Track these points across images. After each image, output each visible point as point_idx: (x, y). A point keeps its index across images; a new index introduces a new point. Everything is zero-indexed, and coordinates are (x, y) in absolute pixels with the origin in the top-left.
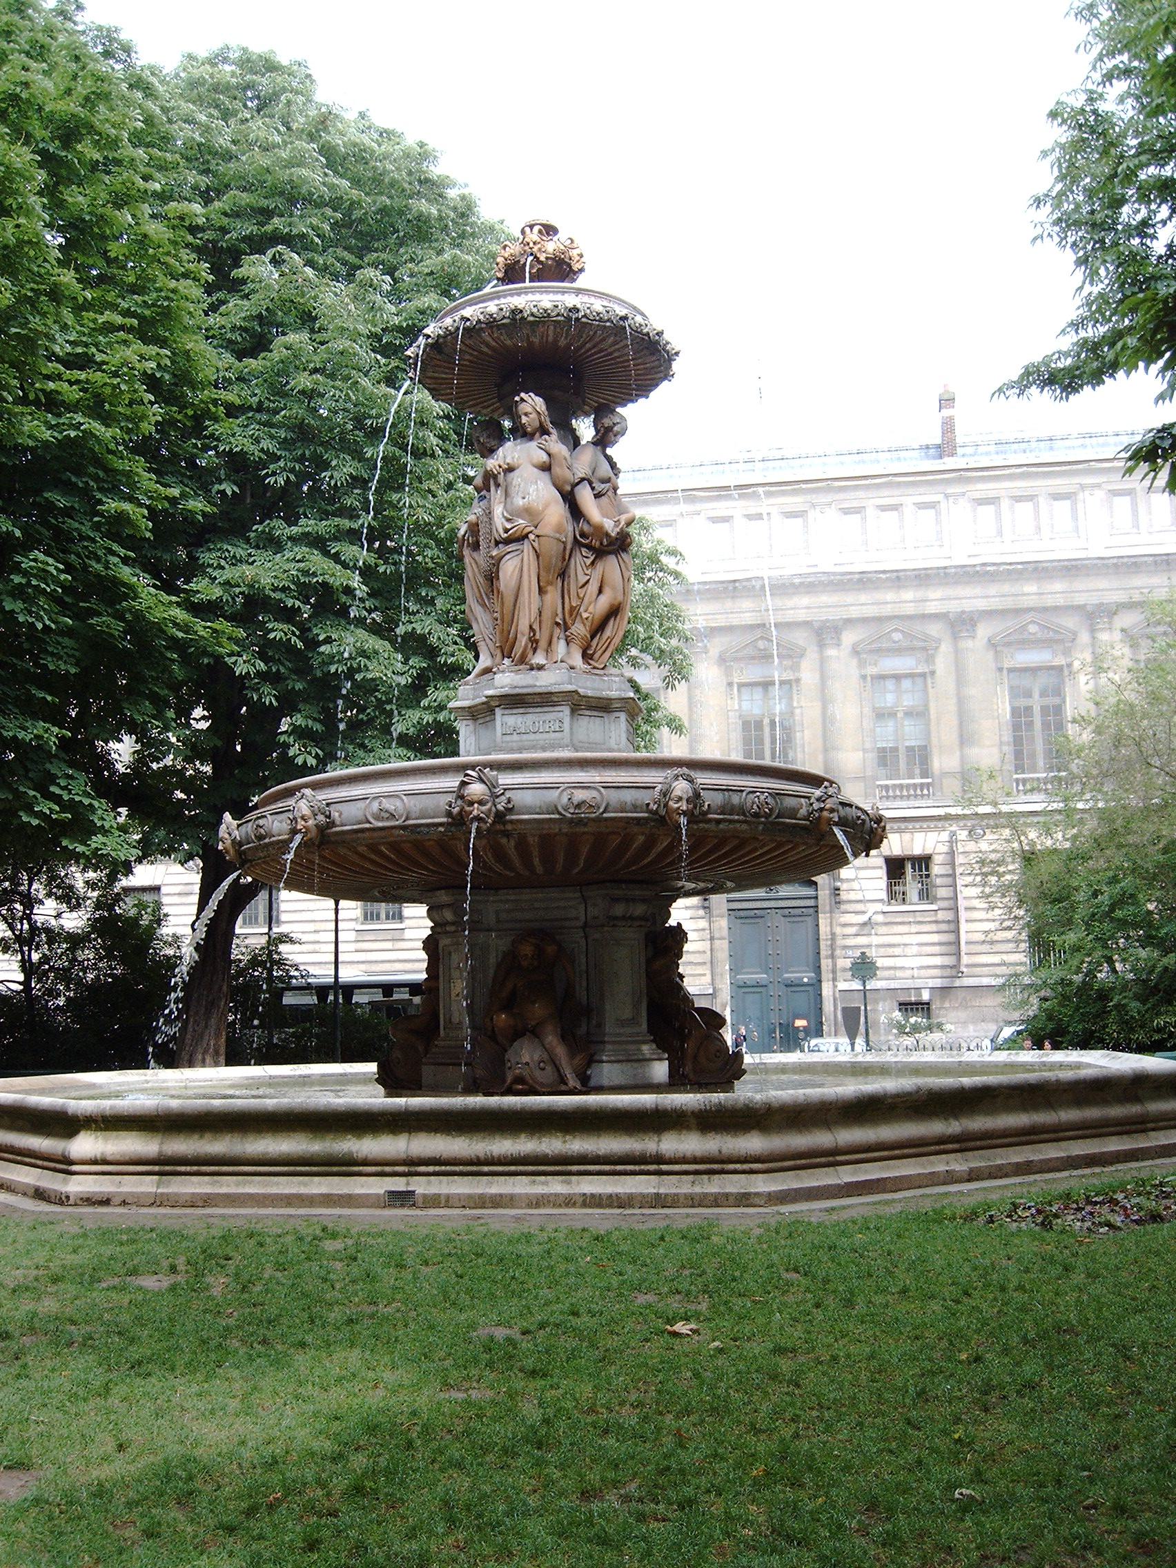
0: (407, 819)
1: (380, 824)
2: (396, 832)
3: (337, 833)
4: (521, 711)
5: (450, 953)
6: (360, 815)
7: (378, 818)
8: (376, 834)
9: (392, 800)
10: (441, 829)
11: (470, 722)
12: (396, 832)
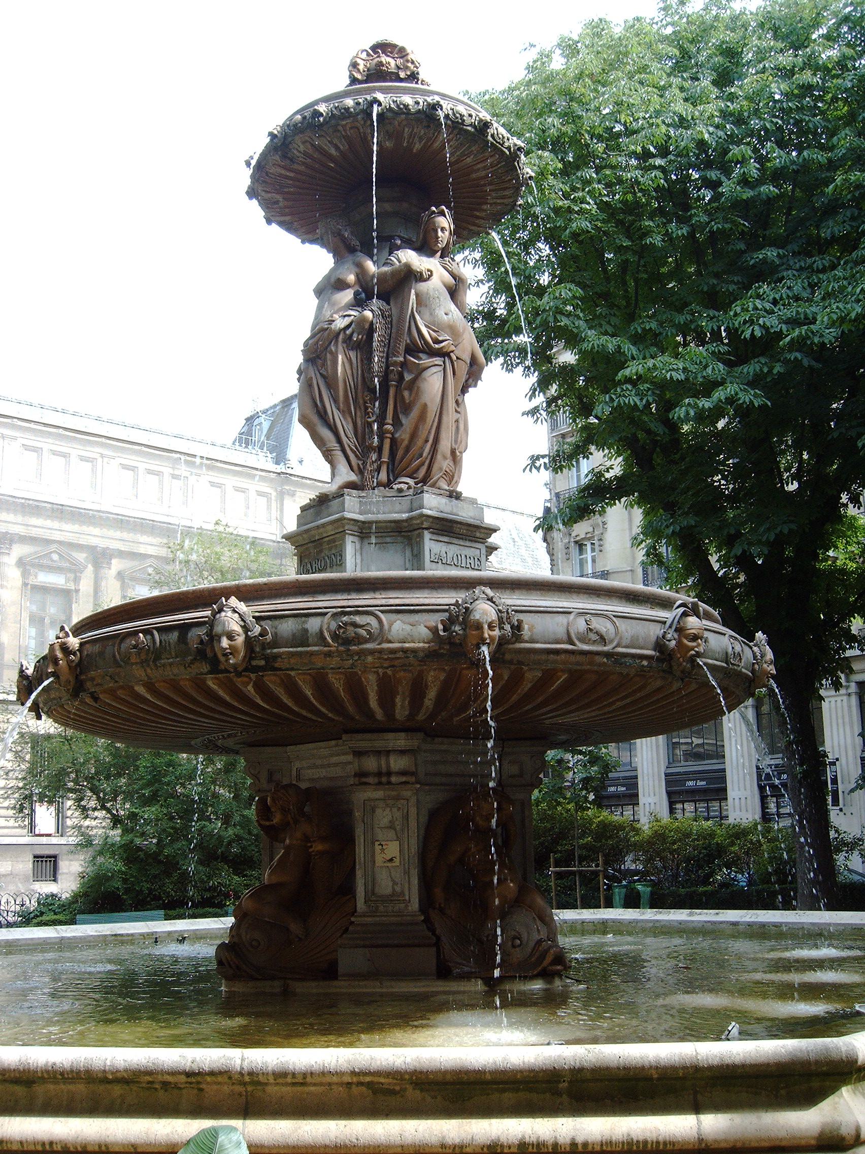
0: (618, 645)
1: (586, 647)
2: (598, 659)
3: (520, 651)
4: (446, 539)
5: (373, 810)
6: (561, 632)
7: (583, 640)
8: (572, 658)
9: (601, 620)
10: (645, 663)
11: (356, 539)
12: (598, 659)
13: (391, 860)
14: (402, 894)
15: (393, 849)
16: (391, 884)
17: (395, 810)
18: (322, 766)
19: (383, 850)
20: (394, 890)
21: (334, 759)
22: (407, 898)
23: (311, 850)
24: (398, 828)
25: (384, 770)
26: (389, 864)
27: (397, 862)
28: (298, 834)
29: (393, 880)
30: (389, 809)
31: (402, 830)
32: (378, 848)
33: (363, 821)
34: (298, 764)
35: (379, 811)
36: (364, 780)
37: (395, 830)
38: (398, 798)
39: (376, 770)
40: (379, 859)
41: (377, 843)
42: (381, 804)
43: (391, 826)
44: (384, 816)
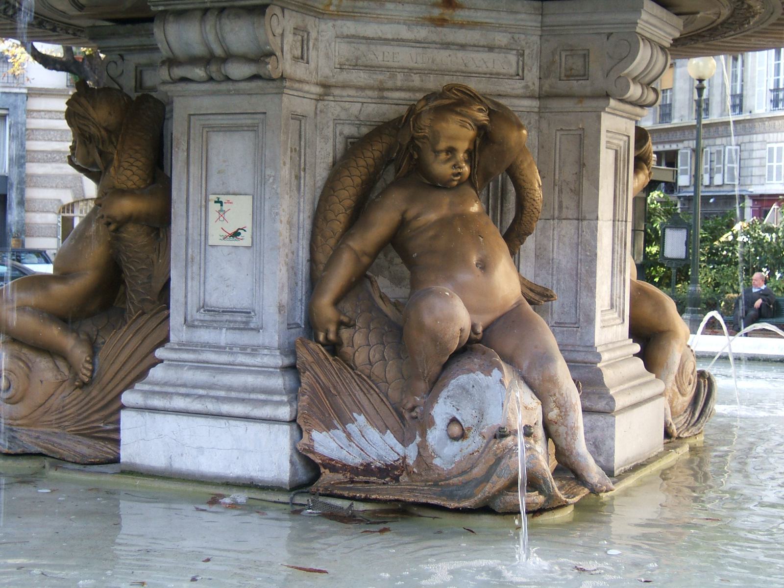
13: (236, 234)
19: (222, 212)
32: (214, 207)
41: (213, 198)
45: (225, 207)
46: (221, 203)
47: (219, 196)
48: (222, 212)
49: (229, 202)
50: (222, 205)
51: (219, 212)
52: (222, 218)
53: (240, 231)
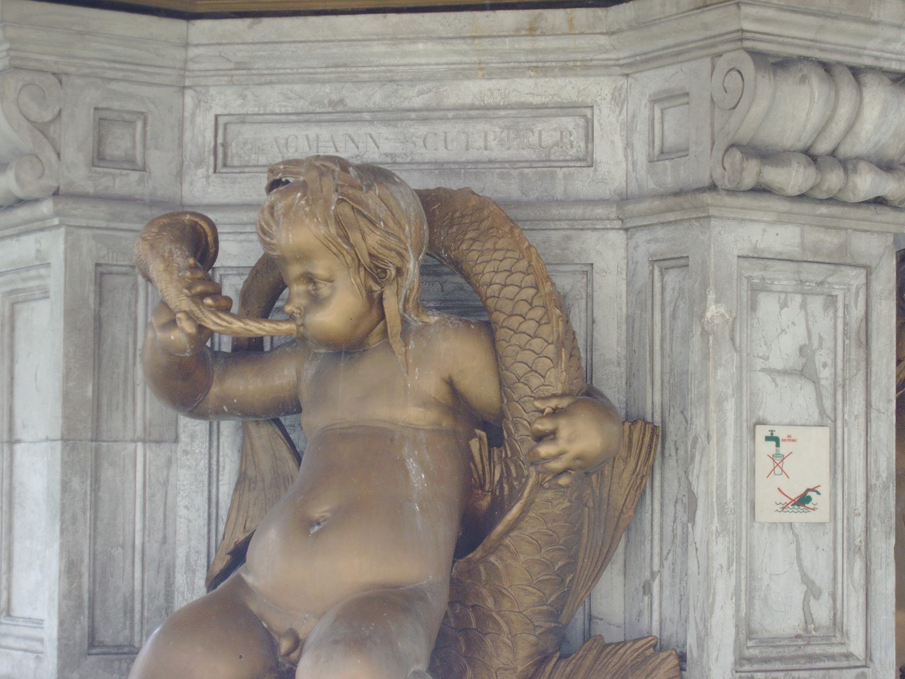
13: (803, 500)
14: (837, 624)
15: (808, 459)
16: (798, 592)
17: (816, 304)
18: (392, 116)
19: (778, 460)
20: (808, 618)
21: (472, 90)
22: (857, 647)
23: (545, 450)
24: (825, 374)
25: (823, 147)
26: (798, 517)
27: (821, 501)
28: (430, 384)
29: (806, 580)
30: (798, 298)
31: (841, 385)
33: (733, 339)
34: (225, 100)
35: (768, 304)
36: (774, 175)
37: (816, 382)
38: (840, 260)
39: (800, 145)
40: (769, 493)
41: (762, 432)
42: (782, 277)
43: (804, 371)
44: (785, 326)
45: (784, 448)
46: (777, 440)
47: (772, 428)
48: (778, 460)
49: (790, 439)
50: (778, 445)
51: (773, 458)
52: (778, 470)
53: (809, 494)
